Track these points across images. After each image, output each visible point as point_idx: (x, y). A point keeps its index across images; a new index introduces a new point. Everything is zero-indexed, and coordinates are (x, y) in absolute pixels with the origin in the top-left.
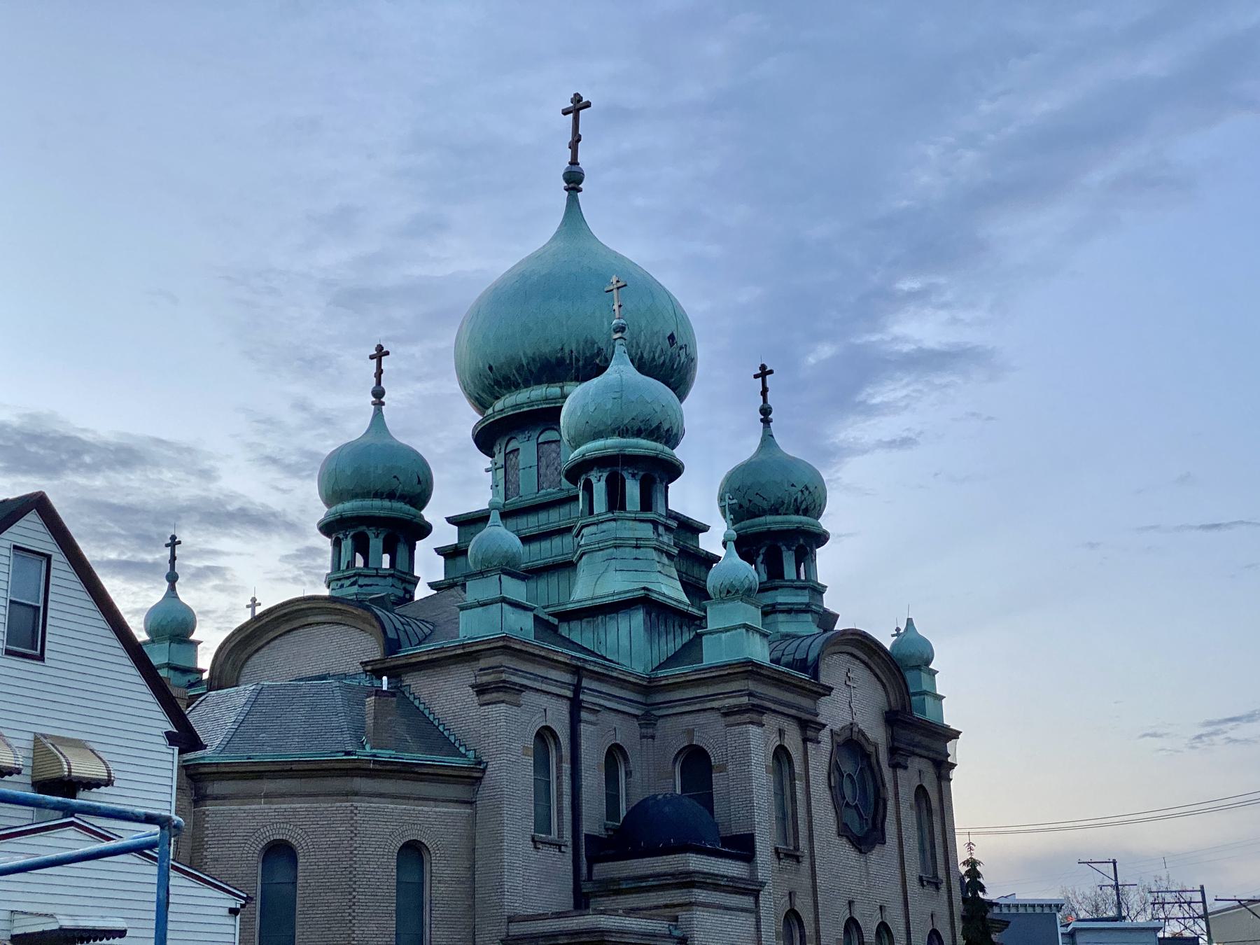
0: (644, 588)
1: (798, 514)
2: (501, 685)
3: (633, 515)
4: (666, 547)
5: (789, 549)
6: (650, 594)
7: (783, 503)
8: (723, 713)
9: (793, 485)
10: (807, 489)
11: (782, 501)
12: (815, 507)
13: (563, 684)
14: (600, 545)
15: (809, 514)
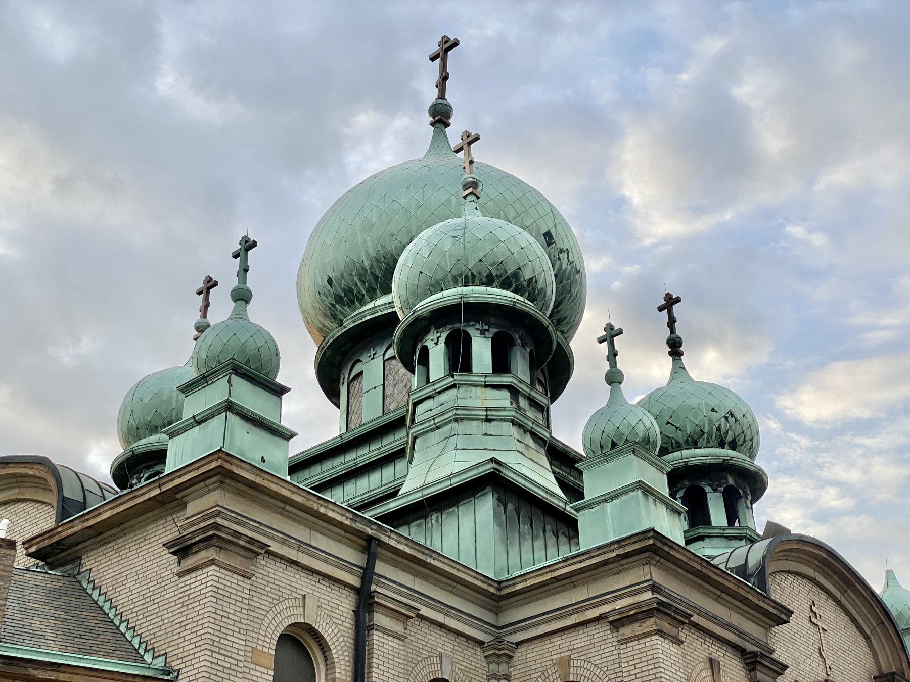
0: (493, 460)
1: (723, 447)
2: (211, 533)
3: (483, 379)
4: (530, 424)
5: (715, 490)
6: (501, 469)
7: (704, 432)
8: (611, 623)
9: (713, 410)
10: (732, 415)
11: (701, 431)
12: (744, 441)
13: (347, 566)
14: (436, 421)
15: (738, 448)
